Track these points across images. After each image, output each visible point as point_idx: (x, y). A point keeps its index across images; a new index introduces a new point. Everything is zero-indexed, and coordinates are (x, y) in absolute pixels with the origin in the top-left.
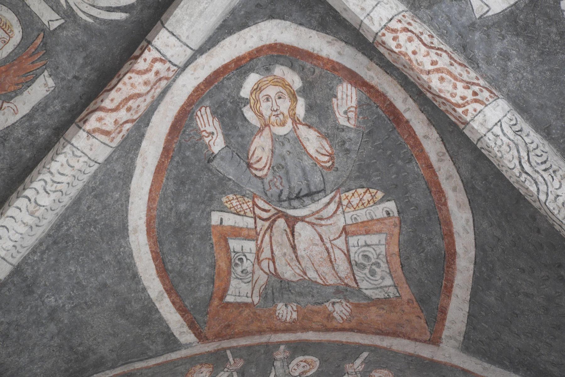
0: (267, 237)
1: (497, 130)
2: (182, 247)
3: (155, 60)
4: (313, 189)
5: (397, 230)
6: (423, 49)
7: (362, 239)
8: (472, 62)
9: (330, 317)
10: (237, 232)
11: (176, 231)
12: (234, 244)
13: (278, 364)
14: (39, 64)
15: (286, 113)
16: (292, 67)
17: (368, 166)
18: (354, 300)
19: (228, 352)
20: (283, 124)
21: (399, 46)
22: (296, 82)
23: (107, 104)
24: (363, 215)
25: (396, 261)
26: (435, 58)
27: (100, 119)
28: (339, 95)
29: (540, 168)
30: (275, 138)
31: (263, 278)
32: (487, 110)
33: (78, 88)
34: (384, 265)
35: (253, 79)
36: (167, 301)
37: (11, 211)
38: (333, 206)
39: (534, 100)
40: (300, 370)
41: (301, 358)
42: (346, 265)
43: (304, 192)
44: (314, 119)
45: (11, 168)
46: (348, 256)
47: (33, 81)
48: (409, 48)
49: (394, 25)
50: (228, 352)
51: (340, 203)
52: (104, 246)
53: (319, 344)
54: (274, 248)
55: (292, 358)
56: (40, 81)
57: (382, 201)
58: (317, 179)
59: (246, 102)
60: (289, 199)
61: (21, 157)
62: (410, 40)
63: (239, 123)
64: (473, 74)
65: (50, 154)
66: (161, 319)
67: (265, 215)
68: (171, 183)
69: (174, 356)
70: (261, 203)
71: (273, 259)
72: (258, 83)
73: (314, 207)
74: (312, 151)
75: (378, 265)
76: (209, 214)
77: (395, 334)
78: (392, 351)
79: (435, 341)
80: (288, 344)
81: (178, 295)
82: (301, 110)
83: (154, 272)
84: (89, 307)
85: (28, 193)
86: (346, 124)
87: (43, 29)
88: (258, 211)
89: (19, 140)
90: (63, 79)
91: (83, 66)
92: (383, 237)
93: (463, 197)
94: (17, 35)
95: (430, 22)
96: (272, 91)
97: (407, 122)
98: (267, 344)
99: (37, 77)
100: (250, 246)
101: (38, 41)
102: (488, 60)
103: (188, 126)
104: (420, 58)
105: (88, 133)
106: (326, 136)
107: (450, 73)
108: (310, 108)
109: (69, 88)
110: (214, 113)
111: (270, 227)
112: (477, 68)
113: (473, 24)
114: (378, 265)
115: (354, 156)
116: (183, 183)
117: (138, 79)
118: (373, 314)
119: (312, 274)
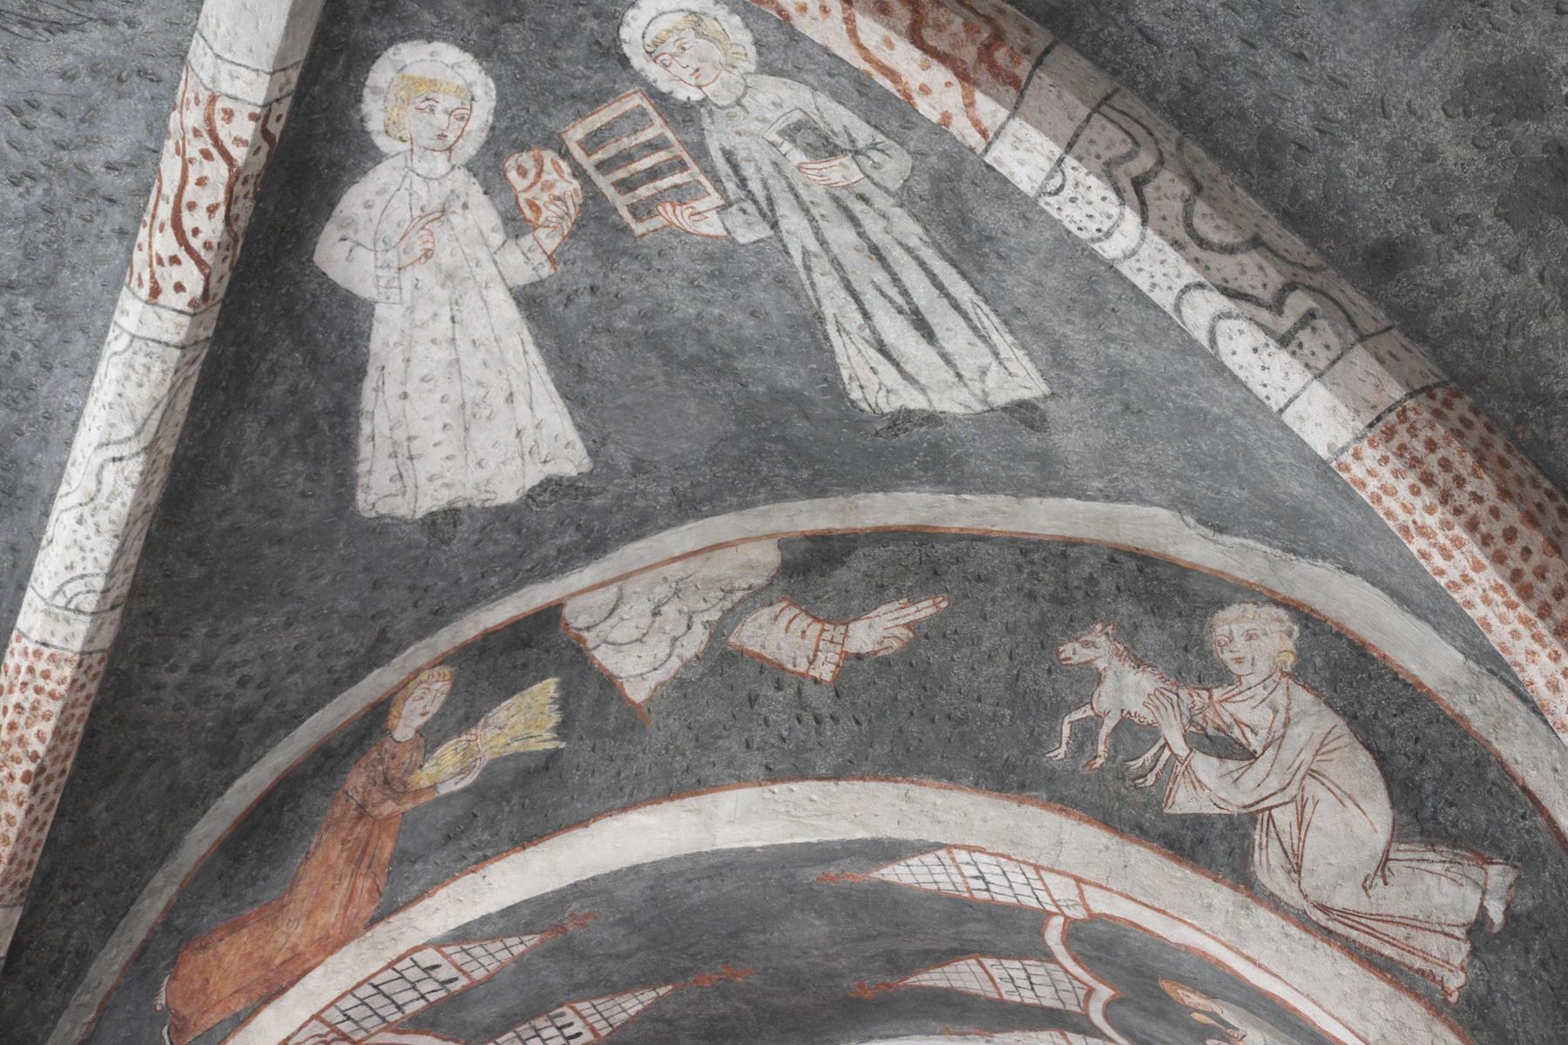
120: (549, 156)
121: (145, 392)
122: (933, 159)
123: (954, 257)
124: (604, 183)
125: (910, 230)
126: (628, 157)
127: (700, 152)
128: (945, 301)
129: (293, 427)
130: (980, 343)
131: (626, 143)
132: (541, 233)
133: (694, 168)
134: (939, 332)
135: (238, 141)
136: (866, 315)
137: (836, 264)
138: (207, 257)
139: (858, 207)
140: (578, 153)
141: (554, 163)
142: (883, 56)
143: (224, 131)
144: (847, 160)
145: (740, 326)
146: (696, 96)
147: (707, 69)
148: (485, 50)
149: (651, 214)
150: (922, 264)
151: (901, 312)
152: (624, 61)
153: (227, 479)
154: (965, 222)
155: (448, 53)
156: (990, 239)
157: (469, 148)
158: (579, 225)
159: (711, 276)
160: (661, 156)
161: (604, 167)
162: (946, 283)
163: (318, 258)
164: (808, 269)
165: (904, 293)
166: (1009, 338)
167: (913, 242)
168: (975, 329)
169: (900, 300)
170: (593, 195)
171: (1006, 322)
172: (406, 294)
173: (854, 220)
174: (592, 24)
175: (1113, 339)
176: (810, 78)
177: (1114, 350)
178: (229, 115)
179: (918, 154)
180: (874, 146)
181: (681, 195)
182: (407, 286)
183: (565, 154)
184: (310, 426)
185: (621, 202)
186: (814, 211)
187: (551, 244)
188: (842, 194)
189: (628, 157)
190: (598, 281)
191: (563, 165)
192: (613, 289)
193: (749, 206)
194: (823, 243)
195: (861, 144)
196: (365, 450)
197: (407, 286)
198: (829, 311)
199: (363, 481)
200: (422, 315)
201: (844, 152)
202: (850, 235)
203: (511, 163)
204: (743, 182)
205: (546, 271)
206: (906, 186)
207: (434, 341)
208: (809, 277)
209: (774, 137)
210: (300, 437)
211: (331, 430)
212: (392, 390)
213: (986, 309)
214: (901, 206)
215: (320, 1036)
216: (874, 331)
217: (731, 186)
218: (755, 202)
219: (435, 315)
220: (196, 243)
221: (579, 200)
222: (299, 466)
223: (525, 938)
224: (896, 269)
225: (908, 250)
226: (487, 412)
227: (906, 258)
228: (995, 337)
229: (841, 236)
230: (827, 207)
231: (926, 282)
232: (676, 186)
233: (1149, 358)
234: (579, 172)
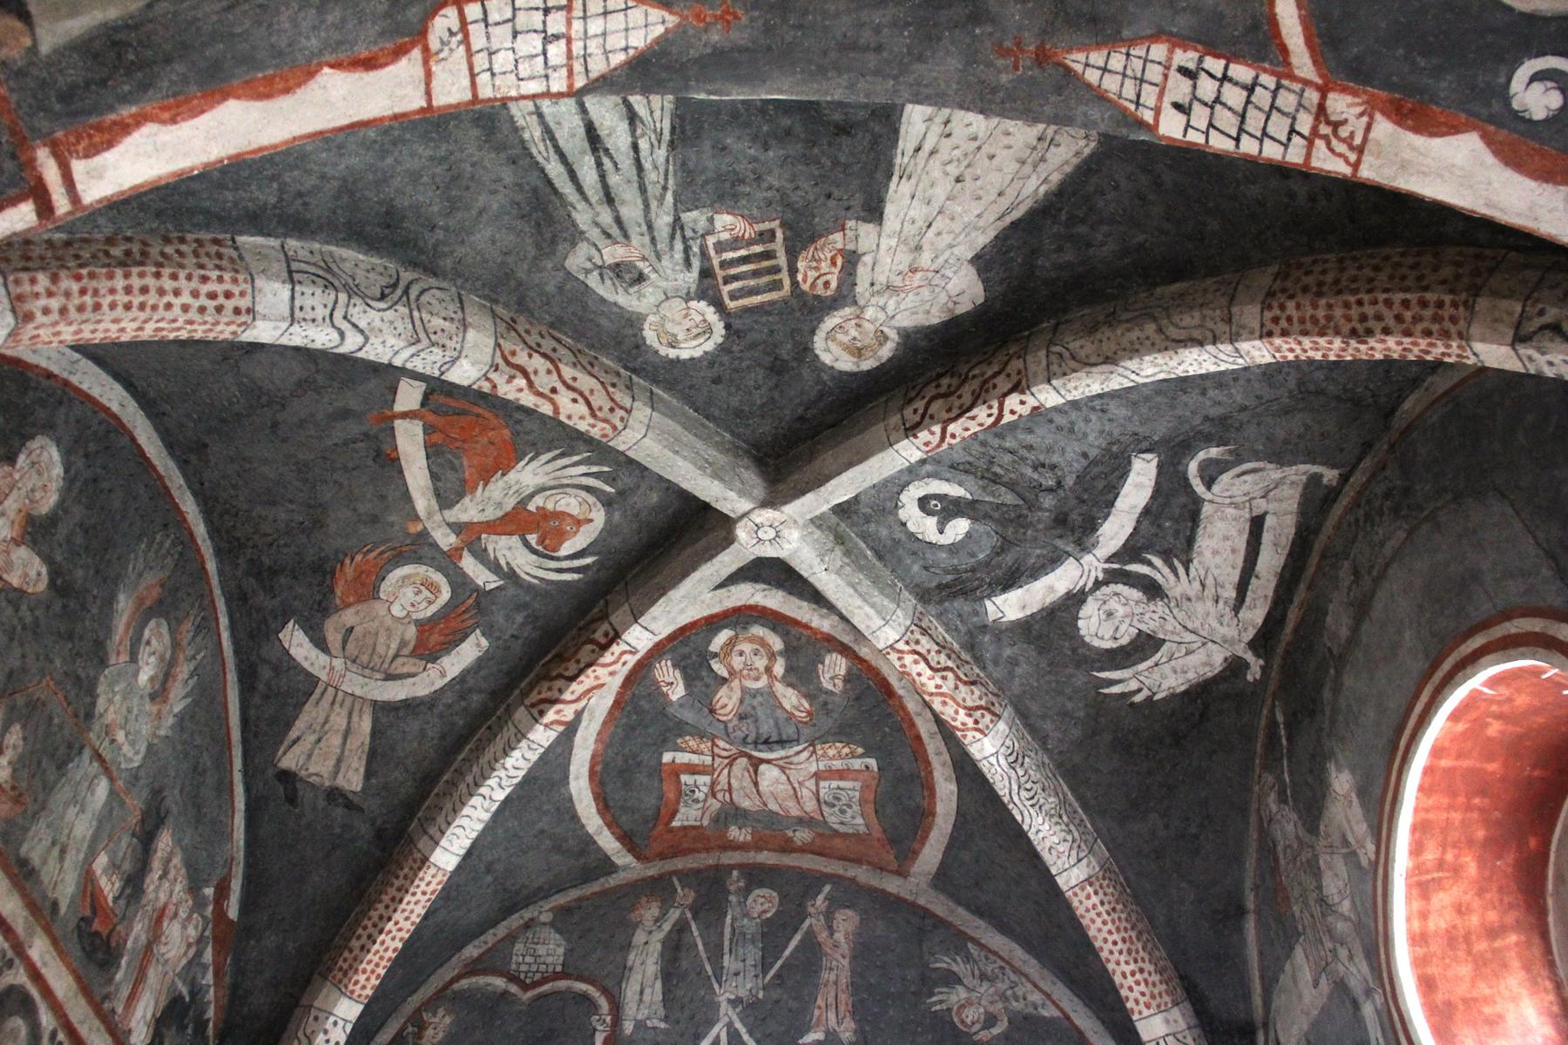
0: (726, 772)
1: (993, 760)
2: (627, 784)
3: (624, 653)
4: (784, 737)
5: (874, 783)
6: (929, 672)
7: (834, 784)
8: (978, 660)
9: (790, 840)
10: (693, 769)
11: (621, 772)
12: (685, 778)
13: (733, 898)
14: (470, 622)
15: (762, 669)
16: (774, 629)
17: (851, 726)
18: (820, 830)
19: (675, 880)
20: (757, 679)
21: (904, 666)
22: (777, 643)
23: (567, 696)
24: (837, 764)
25: (870, 809)
26: (939, 681)
27: (559, 712)
28: (827, 662)
29: (1028, 803)
30: (744, 690)
31: (715, 805)
32: (986, 740)
33: (517, 647)
34: (856, 808)
35: (723, 636)
36: (606, 832)
37: (466, 811)
38: (805, 754)
39: (1034, 708)
40: (759, 908)
41: (757, 892)
42: (814, 802)
43: (774, 738)
44: (793, 680)
45: (443, 737)
46: (817, 795)
47: (463, 640)
48: (914, 669)
49: (901, 646)
50: (675, 880)
51: (814, 752)
52: (544, 798)
53: (775, 870)
54: (733, 781)
55: (747, 891)
56: (472, 639)
57: (861, 756)
58: (790, 731)
59: (715, 655)
60: (756, 743)
61: (453, 724)
62: (916, 662)
63: (704, 673)
64: (977, 671)
65: (499, 743)
66: (599, 849)
67: (725, 754)
68: (619, 730)
69: (613, 881)
70: (721, 744)
71: (730, 790)
72: (731, 639)
73: (782, 753)
74: (788, 707)
75: (850, 806)
76: (661, 755)
77: (858, 861)
78: (858, 884)
79: (902, 873)
80: (740, 866)
81: (618, 826)
82: (779, 668)
83: (594, 810)
84: (525, 853)
85: (483, 790)
86: (830, 687)
87: (477, 589)
88: (716, 750)
89: (449, 706)
90: (499, 638)
91: (523, 624)
92: (858, 785)
93: (950, 771)
94: (446, 594)
95: (939, 616)
96: (747, 647)
97: (900, 697)
98: (717, 868)
99: (466, 636)
100: (707, 779)
101: (471, 601)
102: (996, 663)
103: (644, 678)
104: (924, 679)
105: (546, 726)
106: (808, 696)
107: (954, 700)
108: (789, 670)
109: (507, 648)
110: (674, 666)
111: (730, 765)
112: (984, 668)
113: (985, 626)
114: (850, 806)
115: (835, 715)
116: (633, 729)
117: (601, 671)
118: (838, 843)
119: (773, 806)
120: (805, 287)
121: (1089, 381)
122: (550, 265)
123: (553, 198)
124: (782, 260)
125: (582, 217)
126: (756, 274)
127: (706, 273)
128: (570, 159)
129: (1082, 229)
130: (552, 125)
131: (752, 283)
132: (839, 246)
133: (716, 262)
134: (582, 131)
135: (933, 433)
136: (635, 147)
137: (643, 190)
138: (995, 404)
139: (615, 231)
140: (787, 283)
141: (805, 281)
142: (540, 401)
143: (935, 440)
144: (609, 261)
145: (739, 138)
146: (693, 304)
147: (678, 317)
148: (804, 350)
149: (761, 234)
150: (580, 189)
151: (607, 150)
152: (728, 327)
153: (1141, 245)
154: (538, 224)
155: (826, 358)
156: (523, 217)
157: (847, 311)
158: (813, 239)
159: (742, 181)
160: (733, 271)
161: (777, 270)
162: (565, 176)
163: (981, 300)
164: (665, 188)
165: (599, 164)
166: (526, 136)
167: (581, 206)
168: (553, 139)
169: (606, 161)
170: (792, 255)
171: (526, 149)
172: (947, 255)
173: (618, 221)
174: (735, 348)
175: (444, 159)
176: (615, 309)
177: (442, 152)
178: (926, 444)
179: (561, 267)
180: (587, 272)
181: (735, 243)
182: (941, 260)
183: (795, 284)
184: (1072, 220)
185: (778, 245)
186: (644, 228)
187: (838, 237)
188: (621, 239)
189: (756, 274)
190: (822, 199)
191: (800, 277)
192: (817, 190)
193: (689, 233)
194: (647, 206)
195: (596, 273)
196: (1056, 178)
197: (941, 260)
198: (662, 153)
199: (1075, 161)
200: (947, 239)
201: (610, 267)
202: (625, 212)
203: (829, 293)
204: (687, 250)
205: (851, 224)
206: (574, 244)
207: (952, 219)
208: (666, 179)
209: (653, 276)
210: (1083, 221)
211: (1060, 210)
212: (1004, 203)
213: (540, 159)
214: (582, 233)
215: (1328, 144)
216: (633, 131)
217: (696, 249)
218: (684, 237)
219: (939, 234)
220: (995, 411)
221: (804, 254)
222: (1100, 204)
223: (1078, 68)
224: (599, 186)
225: (585, 198)
226: (956, 152)
227: (590, 193)
228: (537, 133)
229: (631, 211)
230: (633, 231)
231: (580, 174)
232: (735, 249)
233: (413, 155)
234: (793, 271)
